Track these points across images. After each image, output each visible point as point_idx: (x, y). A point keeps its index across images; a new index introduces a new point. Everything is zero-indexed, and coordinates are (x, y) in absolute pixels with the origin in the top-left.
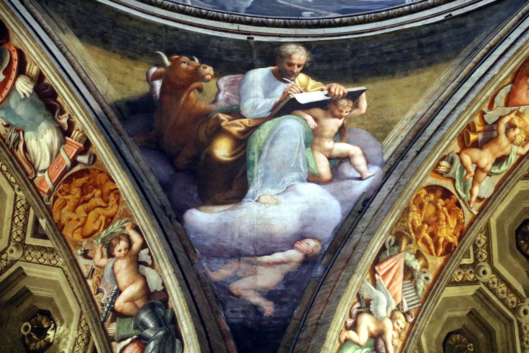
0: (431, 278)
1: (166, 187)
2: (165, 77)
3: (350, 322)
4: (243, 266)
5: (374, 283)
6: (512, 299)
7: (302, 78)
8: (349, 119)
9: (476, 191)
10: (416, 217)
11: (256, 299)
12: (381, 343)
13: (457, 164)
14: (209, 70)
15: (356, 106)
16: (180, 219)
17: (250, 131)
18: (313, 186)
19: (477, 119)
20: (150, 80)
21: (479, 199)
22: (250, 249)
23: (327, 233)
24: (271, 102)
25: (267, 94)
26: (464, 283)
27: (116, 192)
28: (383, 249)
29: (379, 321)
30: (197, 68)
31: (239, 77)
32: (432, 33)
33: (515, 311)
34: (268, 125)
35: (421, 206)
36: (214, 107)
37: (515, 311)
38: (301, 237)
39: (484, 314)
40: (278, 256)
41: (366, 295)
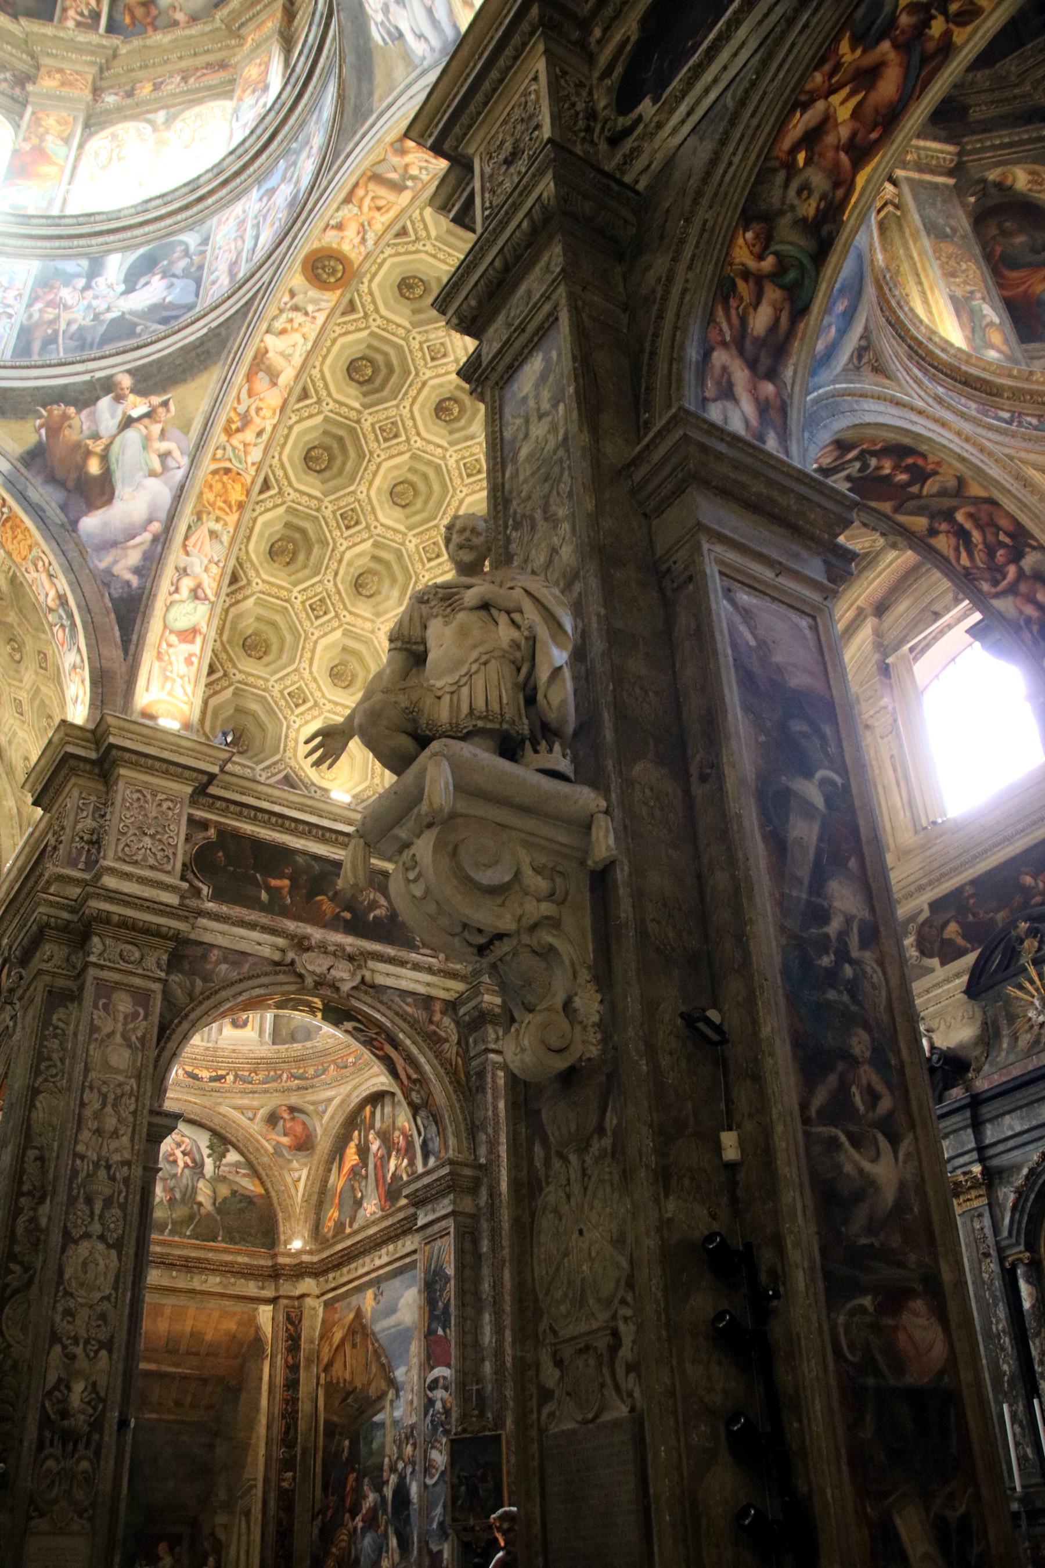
0: (232, 530)
1: (63, 507)
2: (47, 425)
3: (173, 589)
4: (119, 552)
5: (187, 554)
6: (314, 503)
7: (132, 398)
8: (165, 422)
9: (250, 460)
10: (209, 496)
11: (128, 576)
12: (200, 592)
13: (229, 449)
14: (72, 410)
15: (168, 411)
16: (75, 530)
17: (108, 447)
18: (152, 481)
19: (232, 414)
20: (37, 430)
21: (253, 464)
22: (121, 538)
23: (163, 515)
24: (117, 421)
25: (113, 416)
26: (276, 506)
27: (27, 529)
28: (189, 527)
29: (196, 577)
30: (64, 412)
31: (92, 408)
32: (202, 344)
33: (318, 510)
34: (118, 439)
35: (211, 487)
36: (82, 436)
37: (318, 510)
38: (150, 521)
39: (296, 521)
40: (138, 539)
41: (182, 565)
